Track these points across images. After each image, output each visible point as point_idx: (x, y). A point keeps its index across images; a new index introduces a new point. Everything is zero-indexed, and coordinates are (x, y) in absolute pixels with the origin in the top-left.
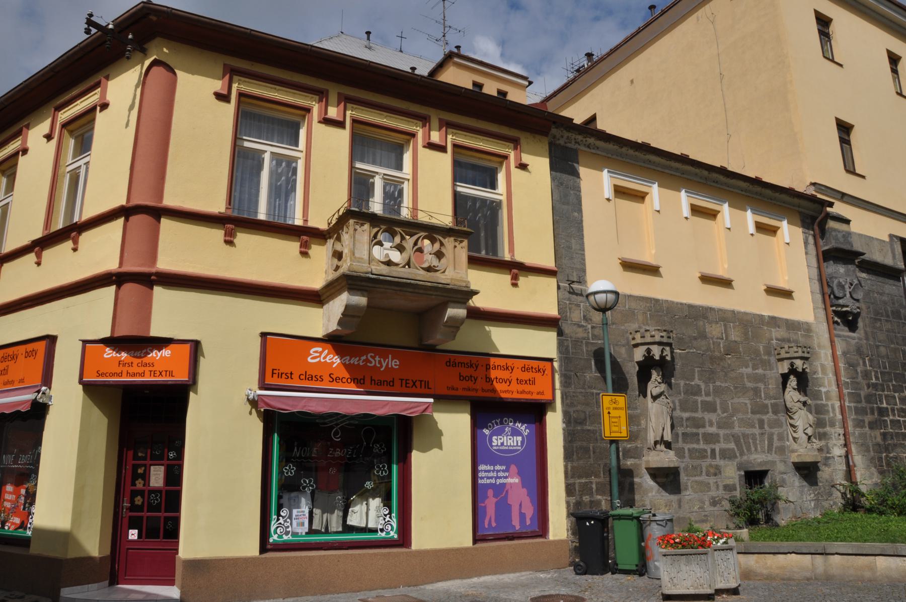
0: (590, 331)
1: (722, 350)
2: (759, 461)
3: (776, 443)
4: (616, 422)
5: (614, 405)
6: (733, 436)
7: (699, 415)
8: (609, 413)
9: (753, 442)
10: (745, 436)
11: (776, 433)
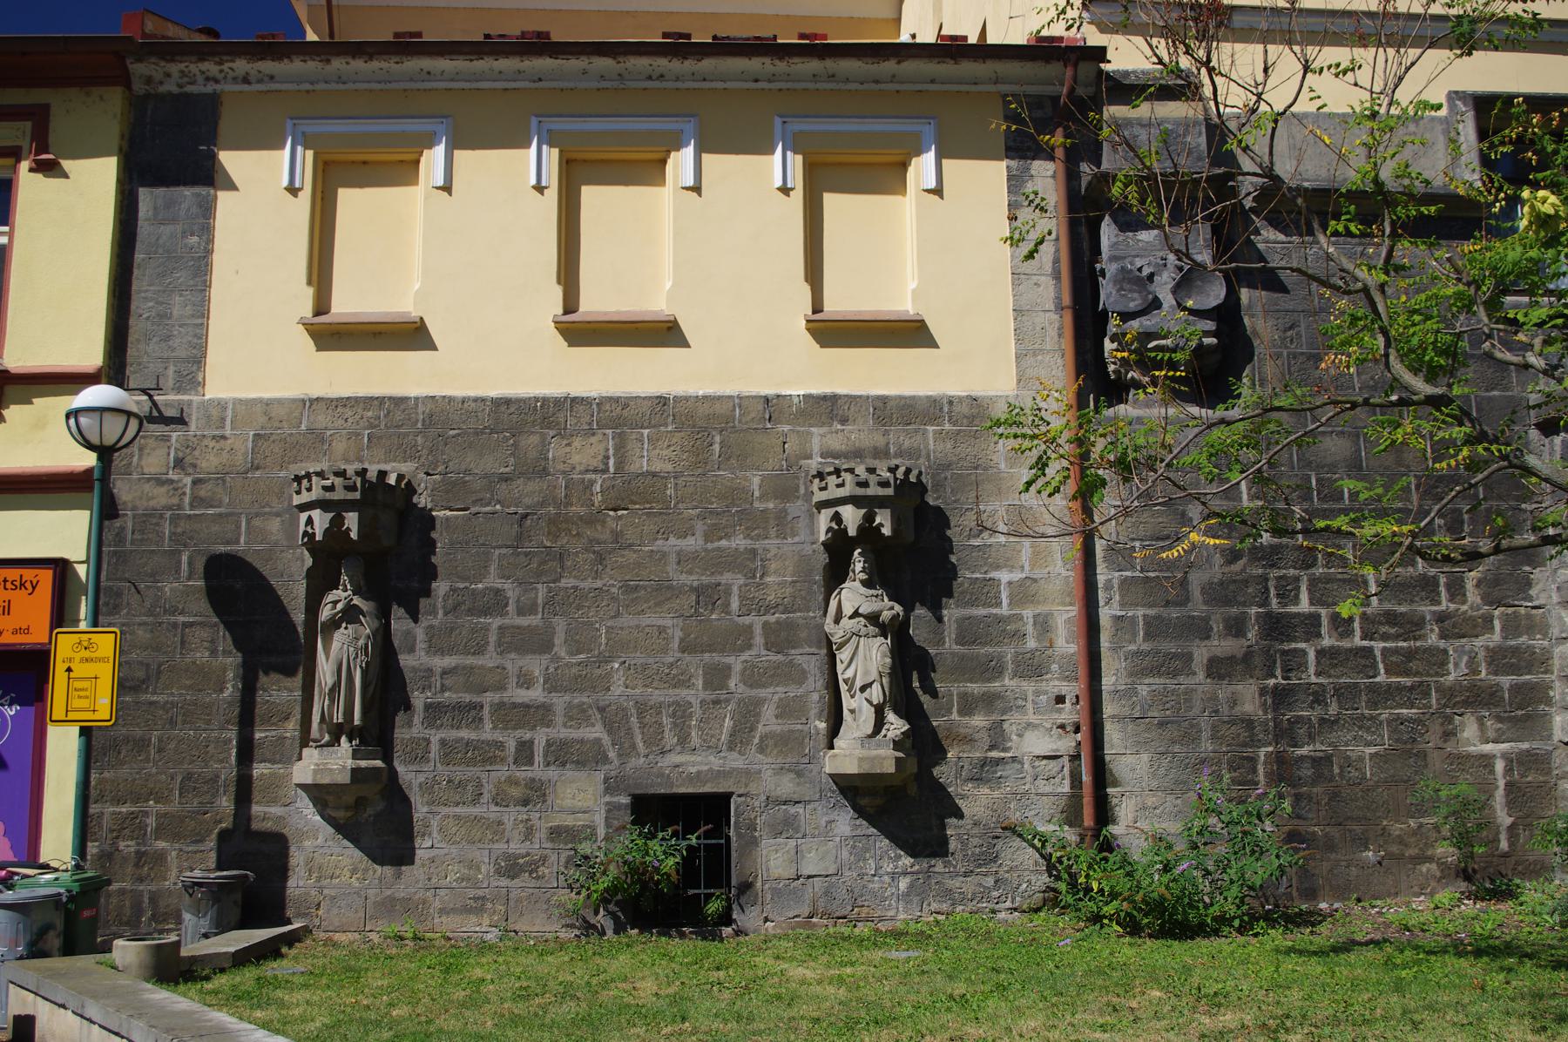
0: (188, 491)
2: (693, 770)
3: (769, 721)
4: (86, 690)
5: (87, 654)
6: (602, 710)
7: (489, 660)
8: (69, 670)
9: (675, 725)
10: (642, 708)
11: (776, 697)
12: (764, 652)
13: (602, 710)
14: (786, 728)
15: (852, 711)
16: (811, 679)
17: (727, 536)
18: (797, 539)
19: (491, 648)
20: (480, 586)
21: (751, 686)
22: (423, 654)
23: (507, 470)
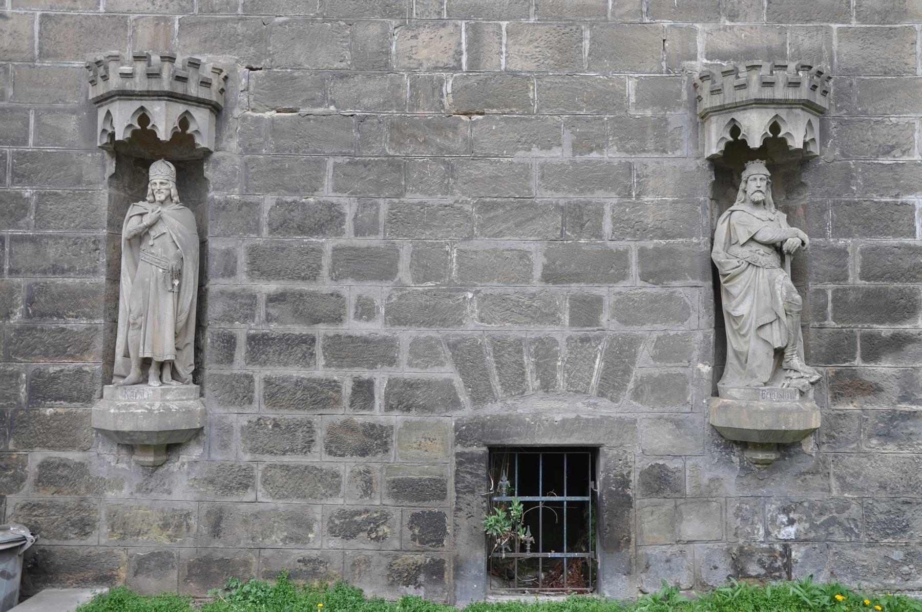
1: (447, 101)
2: (558, 418)
6: (453, 346)
7: (325, 285)
9: (538, 365)
10: (499, 345)
11: (654, 336)
12: (640, 283)
13: (453, 346)
14: (664, 371)
15: (737, 354)
16: (694, 317)
17: (600, 148)
18: (678, 153)
19: (325, 272)
20: (311, 200)
21: (626, 323)
22: (244, 277)
23: (343, 65)
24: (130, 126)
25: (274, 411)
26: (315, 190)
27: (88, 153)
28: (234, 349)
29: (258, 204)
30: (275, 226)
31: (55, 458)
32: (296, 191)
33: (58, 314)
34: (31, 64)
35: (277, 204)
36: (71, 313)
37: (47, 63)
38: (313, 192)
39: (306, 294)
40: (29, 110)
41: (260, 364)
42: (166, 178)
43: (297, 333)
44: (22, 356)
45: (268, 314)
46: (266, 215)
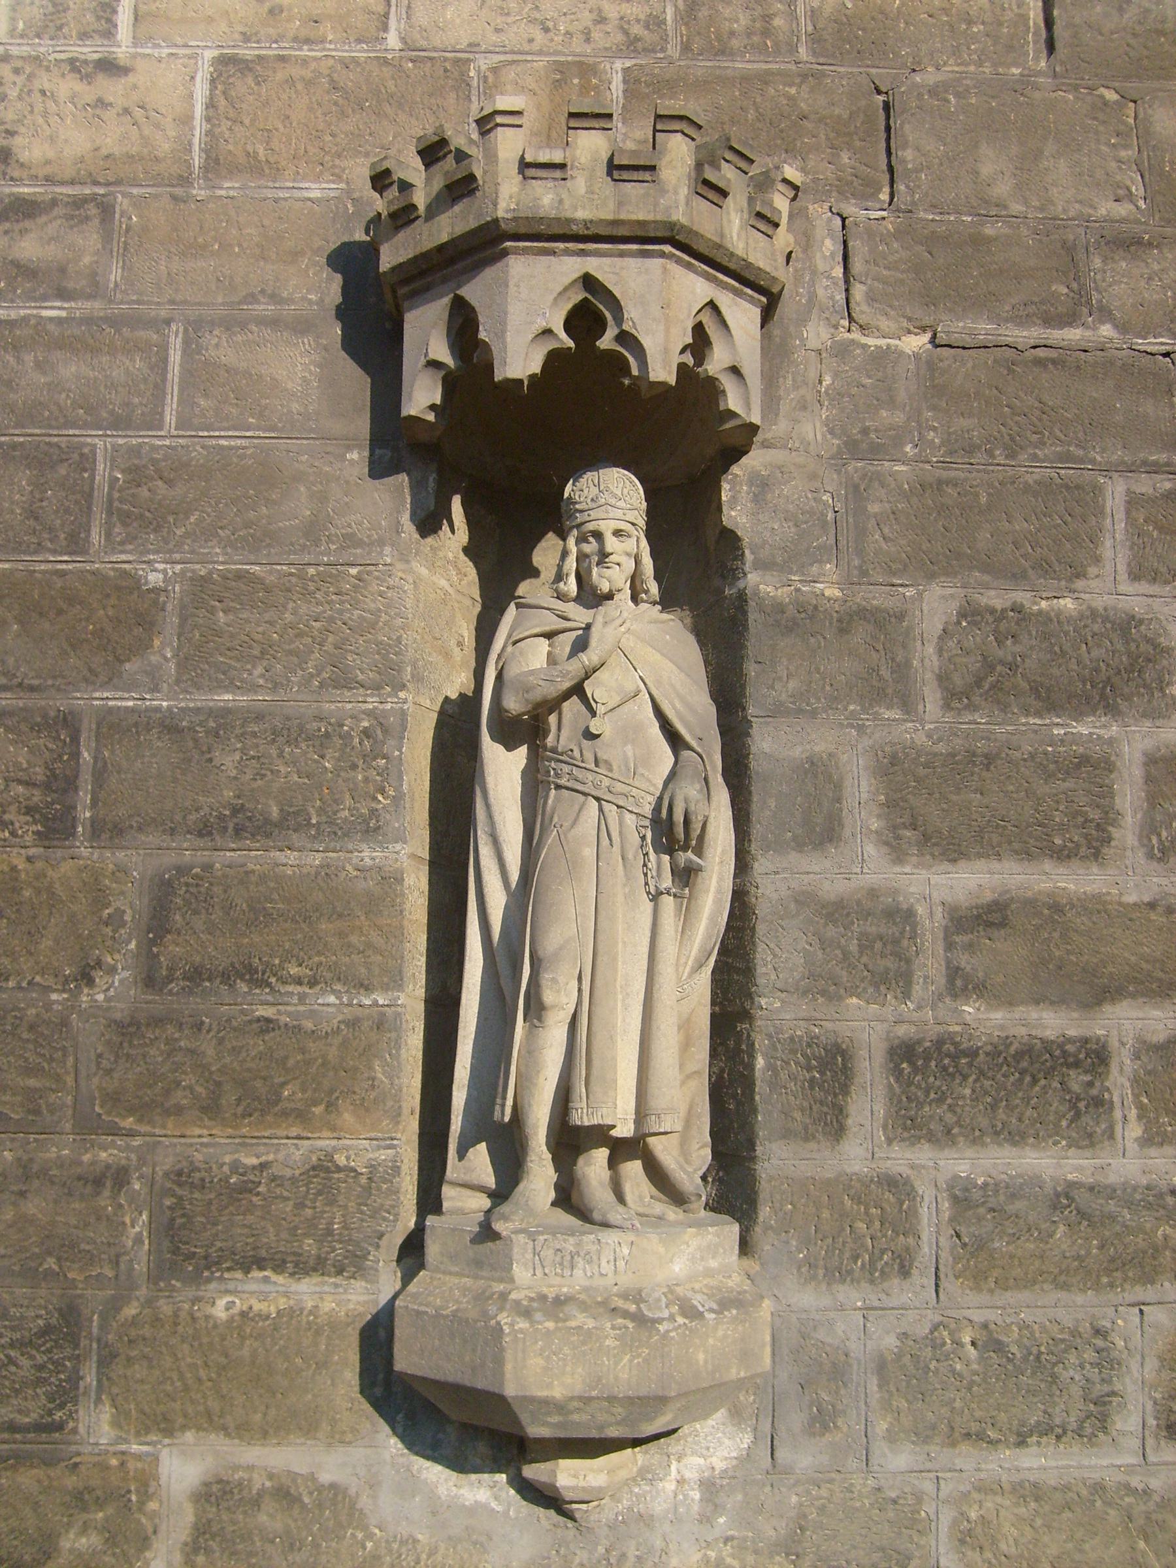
19: (1127, 833)
20: (1068, 604)
23: (1123, 210)
24: (548, 332)
25: (984, 1298)
26: (1078, 576)
27: (349, 448)
28: (845, 1090)
29: (901, 616)
30: (958, 681)
31: (250, 1468)
32: (1017, 577)
33: (252, 971)
34: (178, 191)
35: (962, 615)
36: (294, 970)
37: (229, 187)
38: (1070, 580)
39: (1073, 906)
40: (168, 322)
41: (931, 1138)
42: (631, 516)
43: (1050, 1034)
44: (131, 1111)
45: (953, 972)
46: (930, 650)
